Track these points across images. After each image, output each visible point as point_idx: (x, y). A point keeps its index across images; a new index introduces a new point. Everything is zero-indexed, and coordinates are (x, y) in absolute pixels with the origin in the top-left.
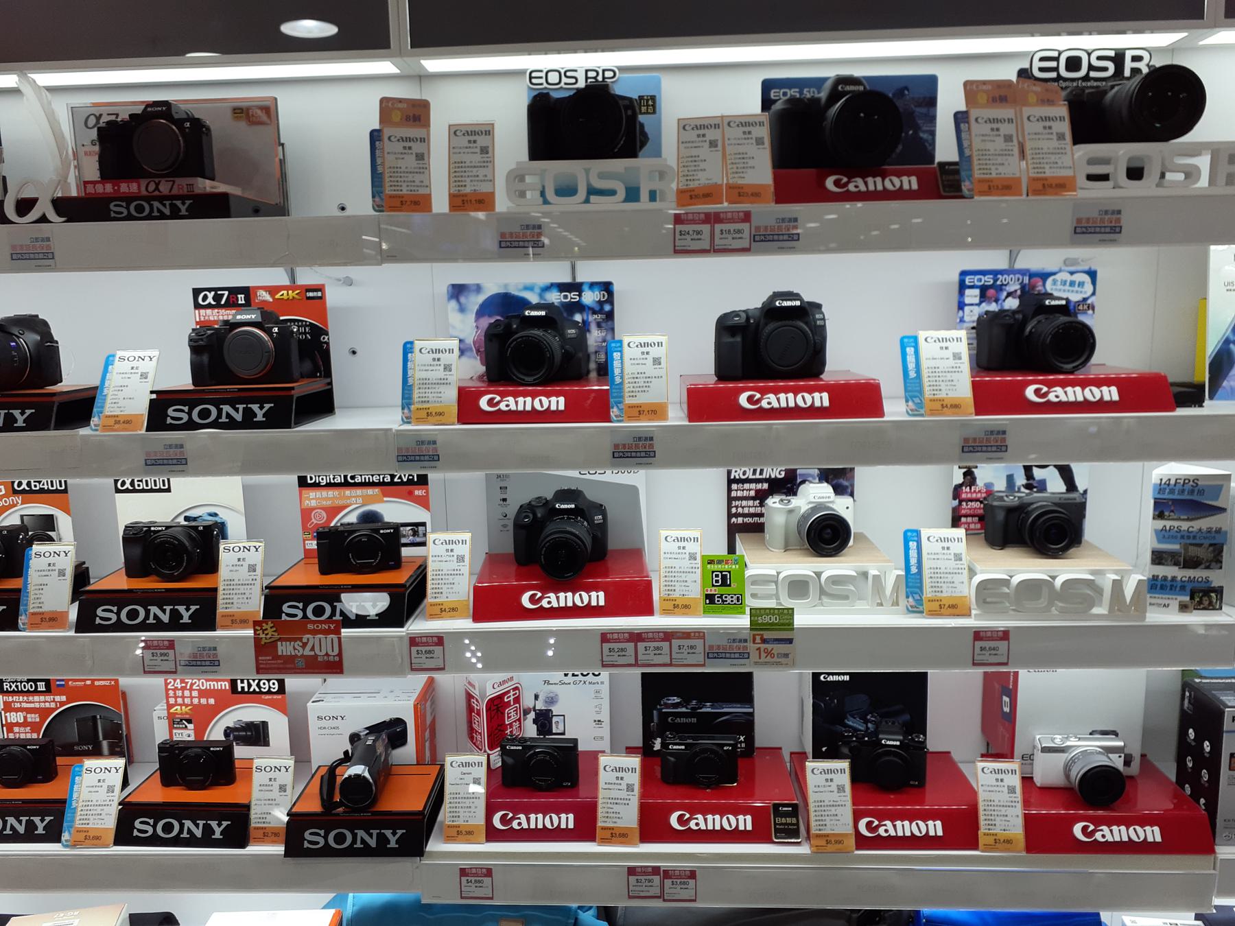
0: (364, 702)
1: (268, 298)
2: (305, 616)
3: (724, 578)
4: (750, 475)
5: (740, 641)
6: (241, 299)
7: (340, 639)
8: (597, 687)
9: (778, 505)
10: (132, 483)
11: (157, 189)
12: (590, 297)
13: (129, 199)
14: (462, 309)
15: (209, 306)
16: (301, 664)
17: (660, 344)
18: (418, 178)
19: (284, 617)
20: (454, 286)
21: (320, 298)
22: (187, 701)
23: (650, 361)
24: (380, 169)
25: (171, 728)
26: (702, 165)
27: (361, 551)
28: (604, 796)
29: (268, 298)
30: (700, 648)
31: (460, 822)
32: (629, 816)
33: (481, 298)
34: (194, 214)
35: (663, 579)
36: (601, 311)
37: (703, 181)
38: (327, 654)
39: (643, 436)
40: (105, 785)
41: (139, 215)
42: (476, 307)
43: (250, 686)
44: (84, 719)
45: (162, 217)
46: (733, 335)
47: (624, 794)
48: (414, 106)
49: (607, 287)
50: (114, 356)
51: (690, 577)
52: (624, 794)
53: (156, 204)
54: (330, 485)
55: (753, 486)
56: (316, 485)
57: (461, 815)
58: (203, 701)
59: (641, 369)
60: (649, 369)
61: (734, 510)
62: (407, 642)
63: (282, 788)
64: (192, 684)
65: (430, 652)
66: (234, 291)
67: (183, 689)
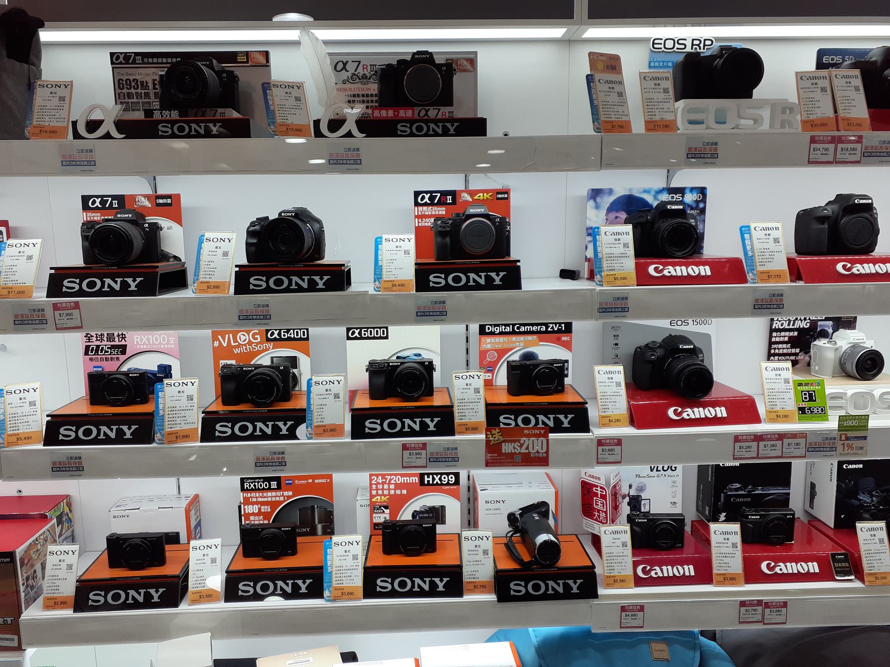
0: (515, 490)
1: (469, 199)
2: (517, 425)
3: (811, 395)
4: (786, 326)
5: (831, 439)
6: (449, 199)
7: (548, 441)
8: (673, 479)
9: (827, 345)
10: (360, 333)
11: (426, 114)
12: (689, 198)
13: (411, 122)
14: (597, 207)
15: (426, 204)
16: (518, 459)
17: (777, 229)
18: (620, 109)
19: (502, 426)
20: (593, 190)
21: (507, 198)
22: (386, 492)
23: (771, 241)
24: (596, 102)
25: (372, 513)
26: (818, 104)
27: (535, 380)
28: (716, 551)
29: (469, 199)
30: (803, 445)
31: (615, 573)
32: (736, 565)
33: (612, 199)
34: (459, 133)
35: (767, 398)
36: (697, 208)
37: (819, 115)
38: (538, 452)
39: (777, 293)
40: (351, 555)
41: (419, 133)
42: (608, 205)
43: (434, 479)
44: (306, 509)
45: (436, 134)
46: (823, 224)
47: (731, 550)
48: (610, 59)
49: (702, 191)
50: (381, 238)
51: (786, 396)
52: (731, 550)
53: (432, 125)
54: (501, 333)
55: (787, 334)
56: (492, 334)
57: (616, 568)
58: (398, 492)
59: (766, 246)
60: (772, 246)
61: (772, 351)
62: (595, 443)
63: (485, 552)
64: (390, 480)
65: (612, 450)
66: (444, 193)
67: (383, 483)
